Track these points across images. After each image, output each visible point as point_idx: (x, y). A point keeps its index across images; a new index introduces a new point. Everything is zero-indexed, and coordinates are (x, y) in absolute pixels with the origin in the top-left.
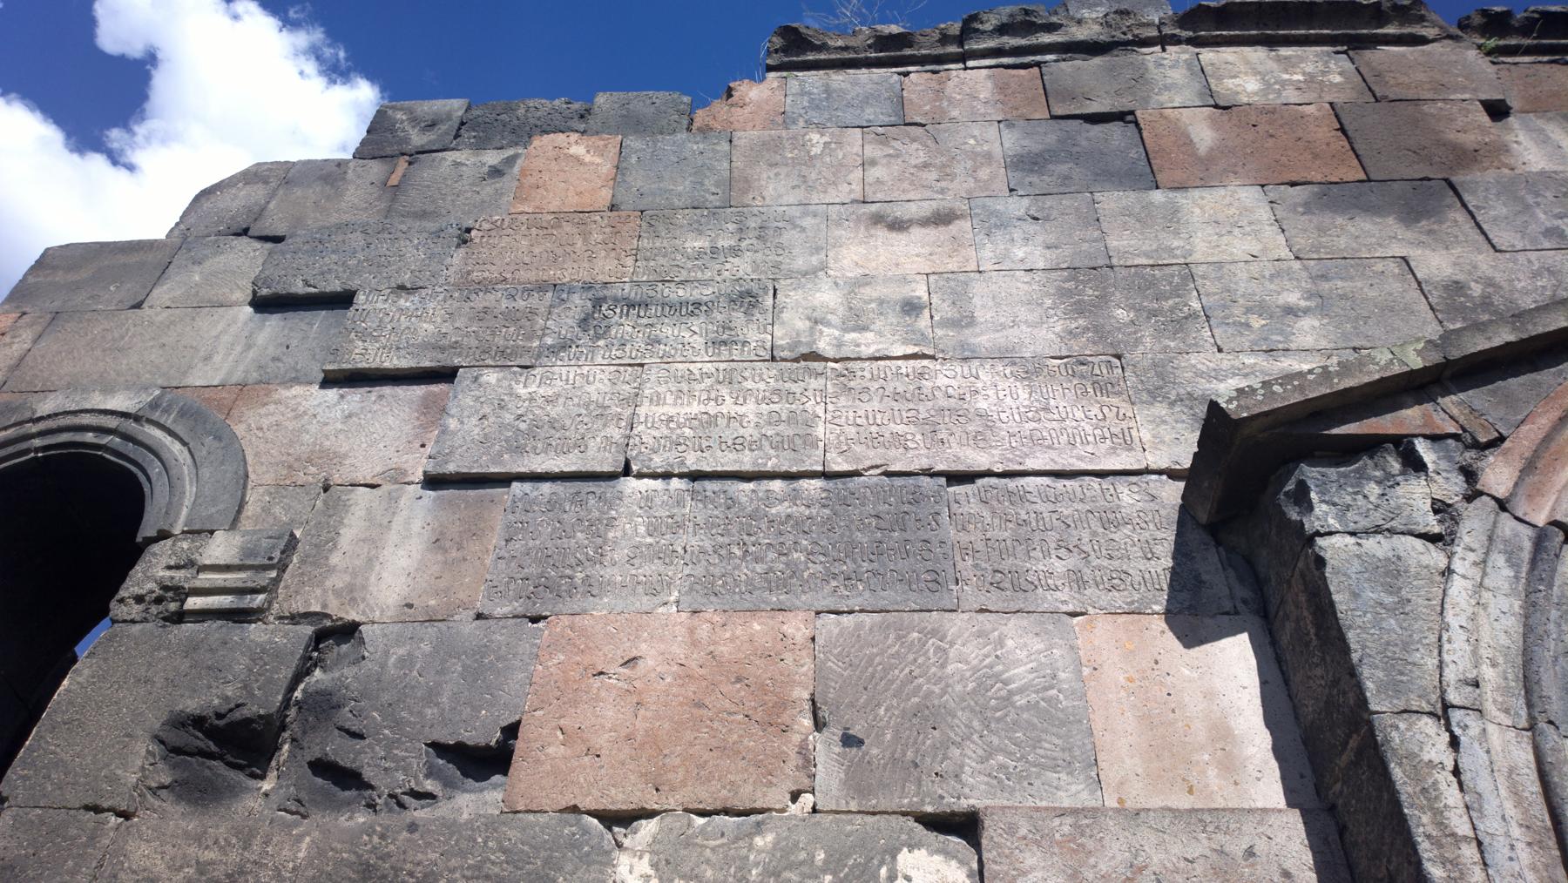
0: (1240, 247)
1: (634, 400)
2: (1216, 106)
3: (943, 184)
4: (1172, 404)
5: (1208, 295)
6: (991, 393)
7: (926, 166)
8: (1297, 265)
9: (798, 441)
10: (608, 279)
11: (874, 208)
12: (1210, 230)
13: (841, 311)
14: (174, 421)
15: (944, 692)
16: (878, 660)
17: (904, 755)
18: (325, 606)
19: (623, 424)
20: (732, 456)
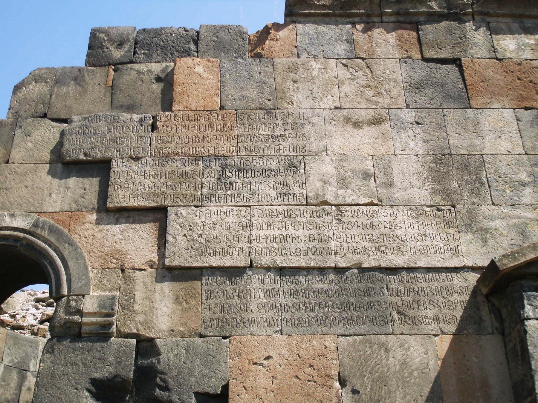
0: (504, 146)
1: (250, 226)
2: (497, 59)
3: (376, 99)
4: (474, 233)
5: (490, 174)
6: (402, 225)
7: (367, 86)
8: (525, 157)
9: (323, 251)
10: (226, 154)
11: (345, 112)
12: (492, 136)
13: (335, 175)
14: (48, 235)
15: (388, 370)
16: (362, 357)
17: (375, 397)
18: (138, 330)
19: (246, 240)
20: (296, 258)
